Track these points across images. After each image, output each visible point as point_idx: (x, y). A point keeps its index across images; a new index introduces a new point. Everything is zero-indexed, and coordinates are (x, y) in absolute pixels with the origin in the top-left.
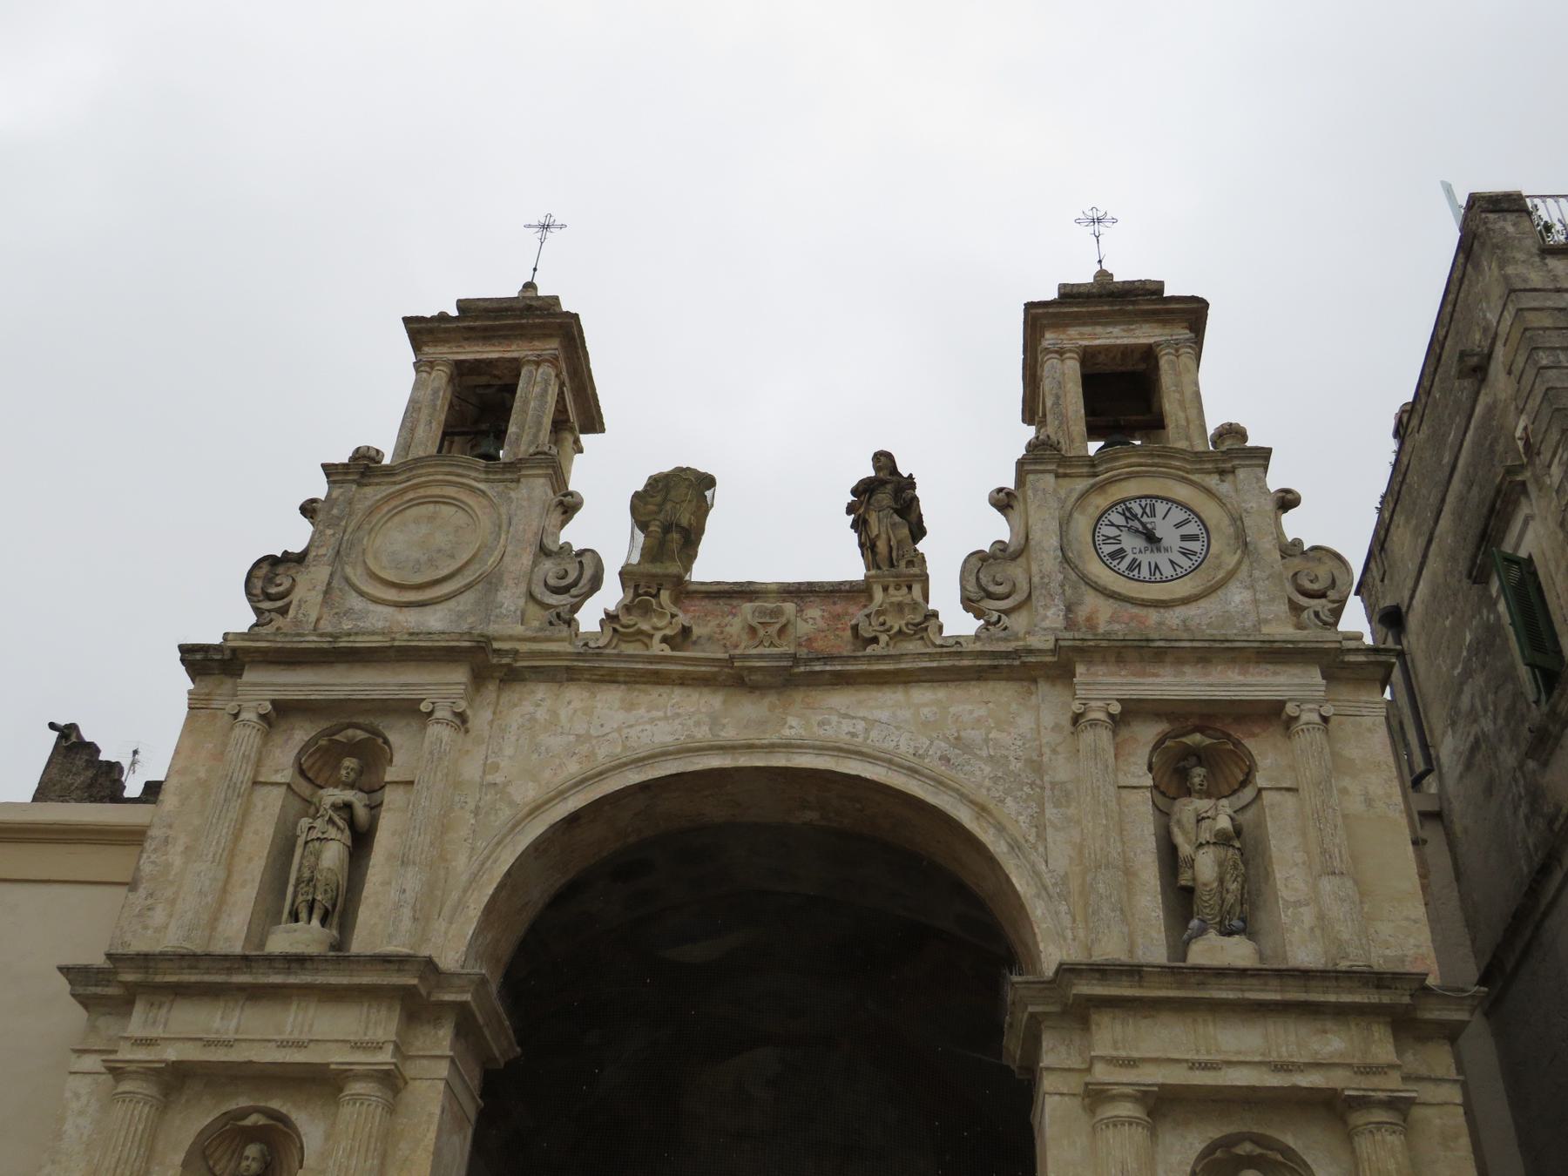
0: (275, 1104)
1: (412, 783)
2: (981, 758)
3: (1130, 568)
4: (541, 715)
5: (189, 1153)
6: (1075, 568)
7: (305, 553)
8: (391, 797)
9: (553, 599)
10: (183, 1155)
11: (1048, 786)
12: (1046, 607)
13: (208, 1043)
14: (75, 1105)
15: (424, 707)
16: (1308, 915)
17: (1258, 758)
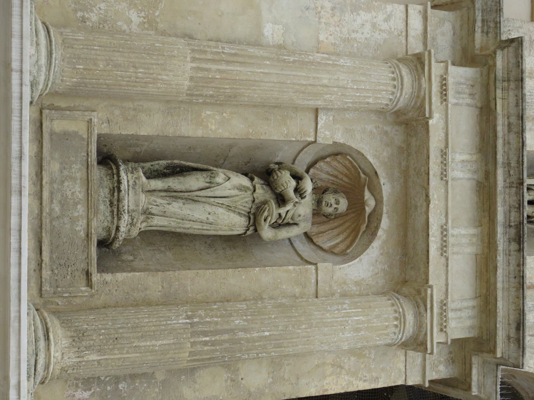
0: (385, 223)
5: (342, 145)
10: (341, 141)
13: (444, 154)
14: (381, 17)
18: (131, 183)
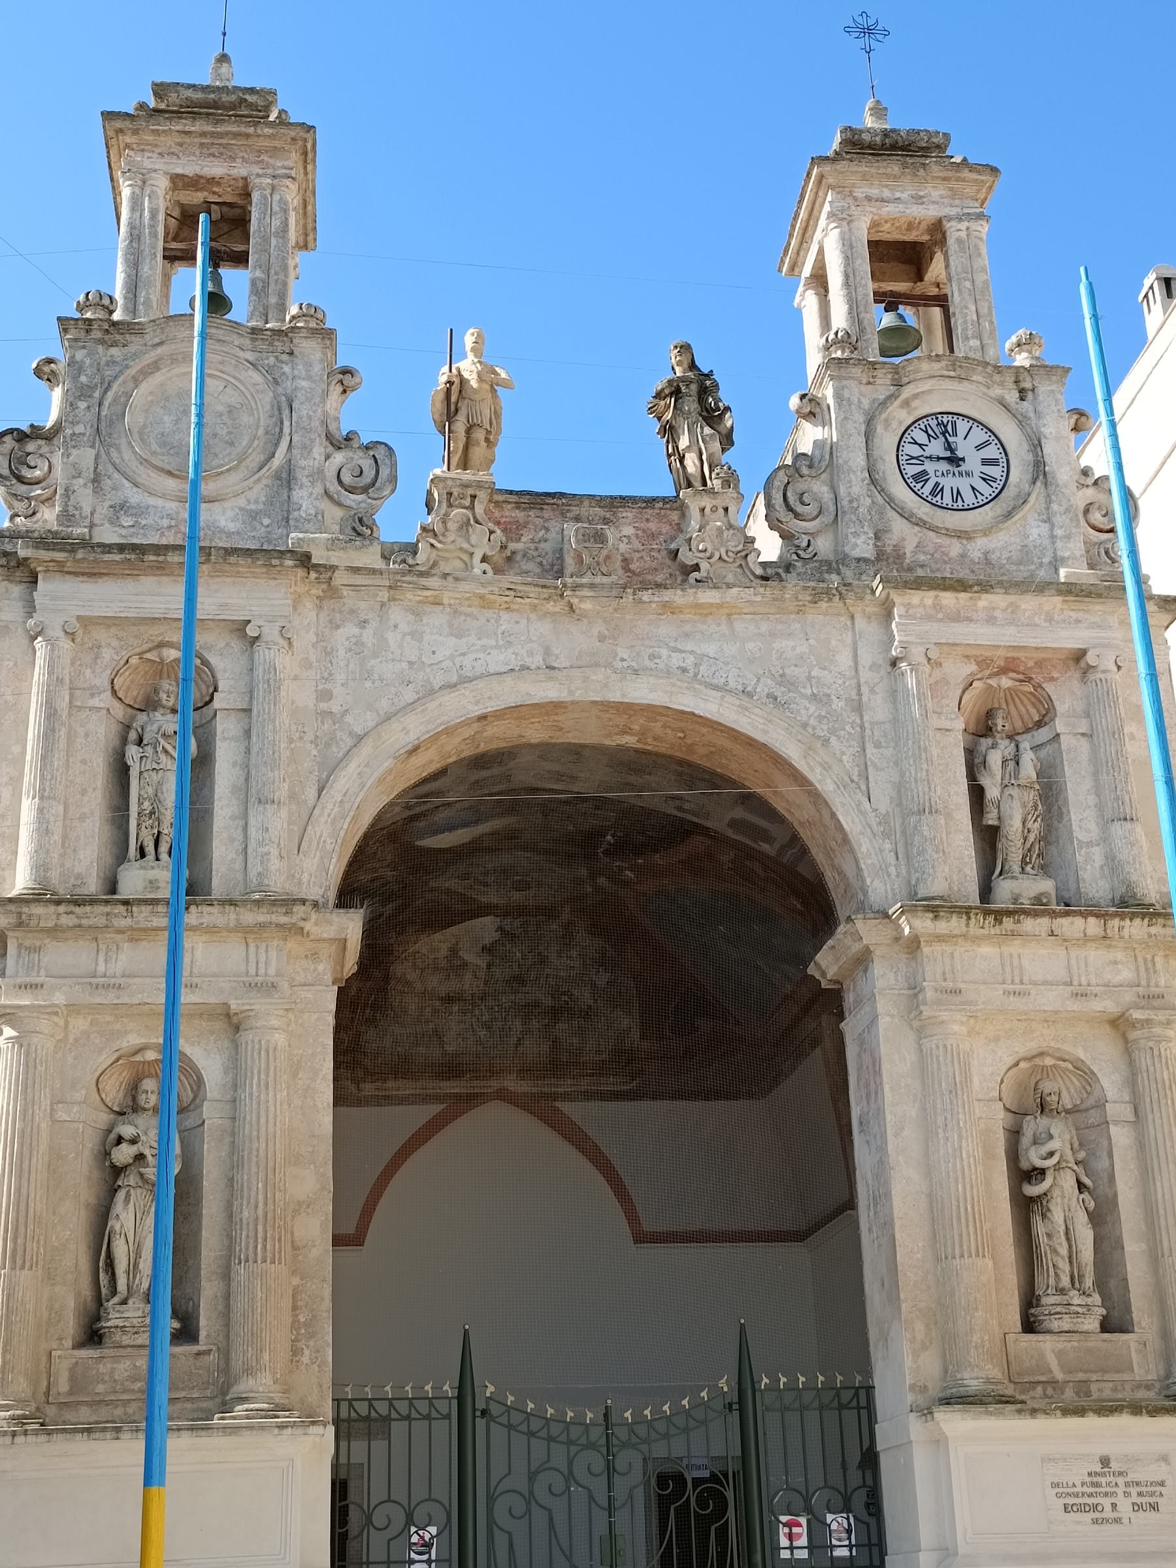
2: (804, 696)
3: (933, 493)
4: (368, 636)
6: (882, 491)
7: (57, 429)
8: (226, 729)
9: (352, 499)
11: (867, 725)
12: (856, 534)
15: (251, 631)
16: (1098, 854)
17: (1056, 703)
18: (118, 1315)
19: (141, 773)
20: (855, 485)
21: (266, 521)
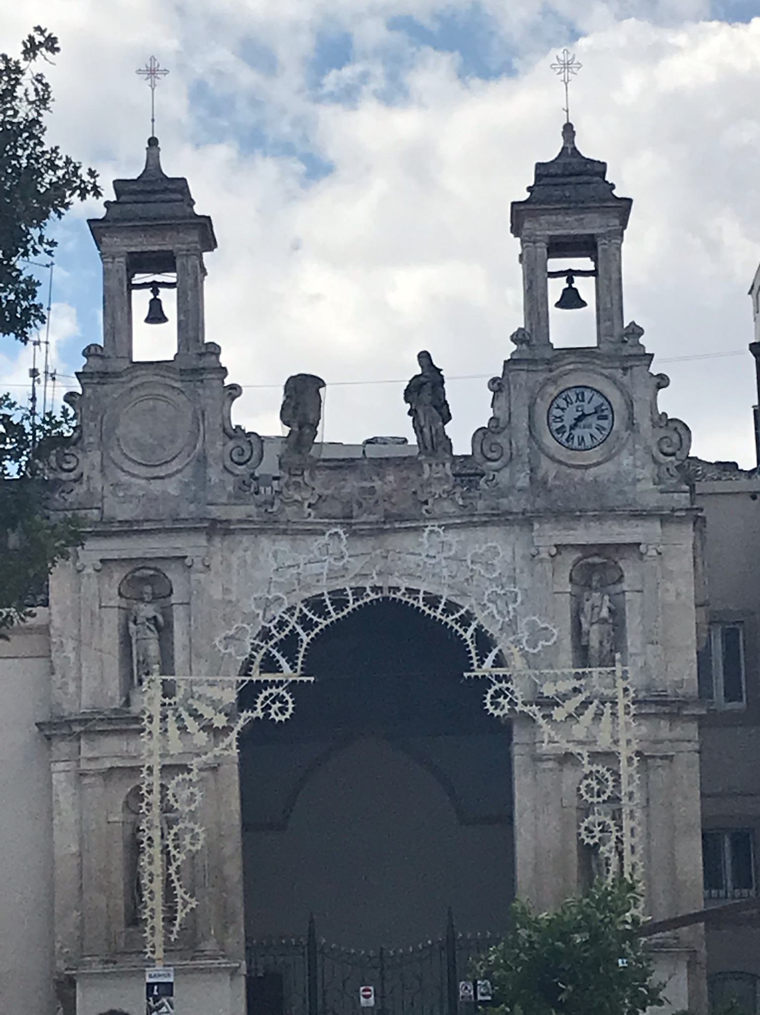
1: (188, 604)
3: (567, 440)
8: (178, 613)
19: (137, 640)
20: (521, 440)
21: (193, 488)
